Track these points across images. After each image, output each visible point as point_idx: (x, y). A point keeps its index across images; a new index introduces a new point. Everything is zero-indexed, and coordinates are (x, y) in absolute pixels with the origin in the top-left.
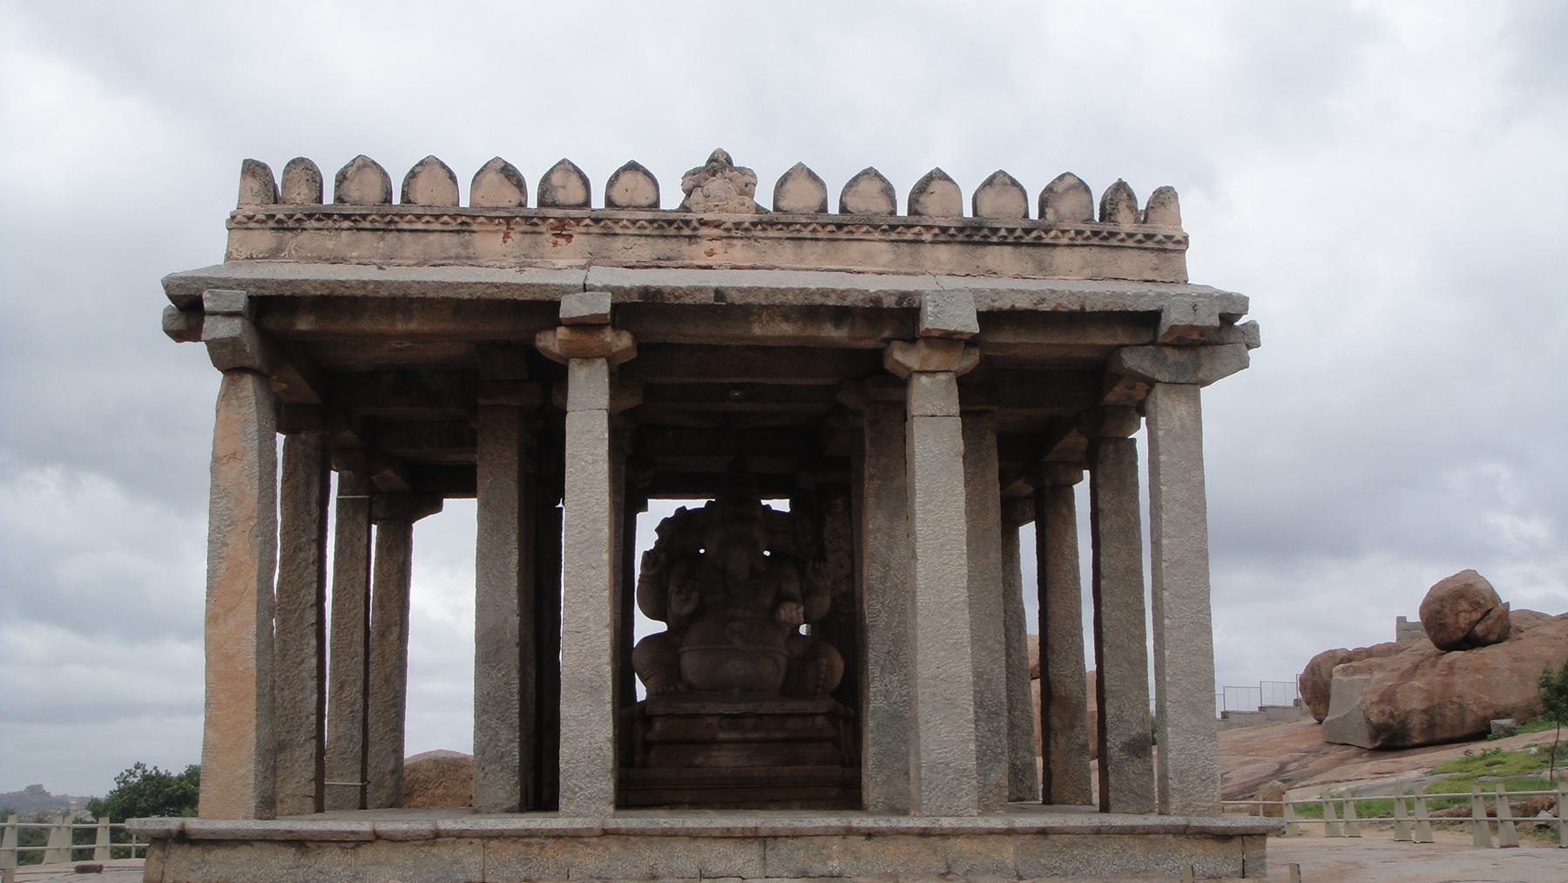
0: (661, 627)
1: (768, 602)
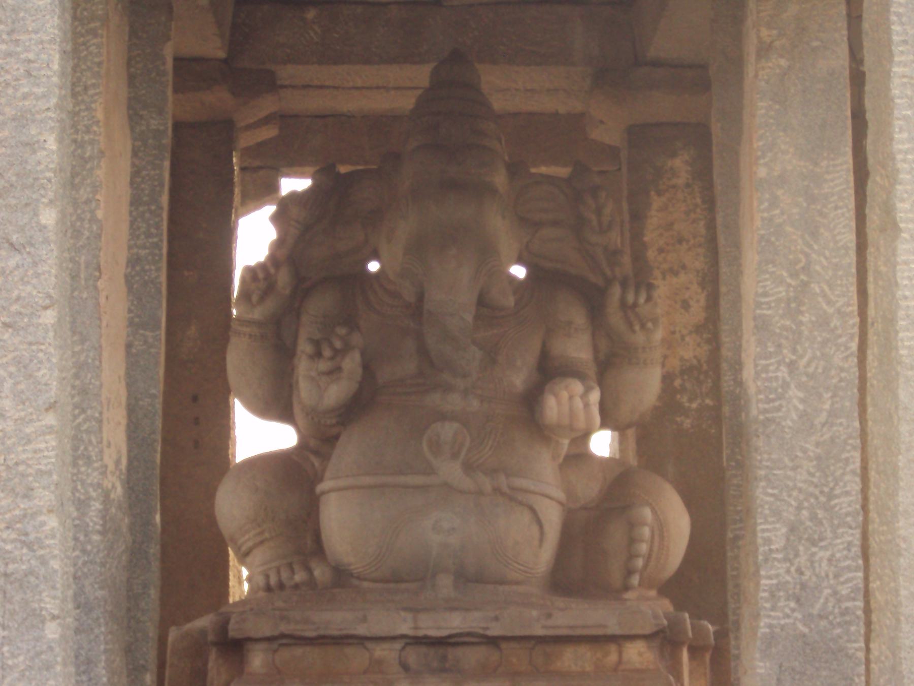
1: (519, 379)
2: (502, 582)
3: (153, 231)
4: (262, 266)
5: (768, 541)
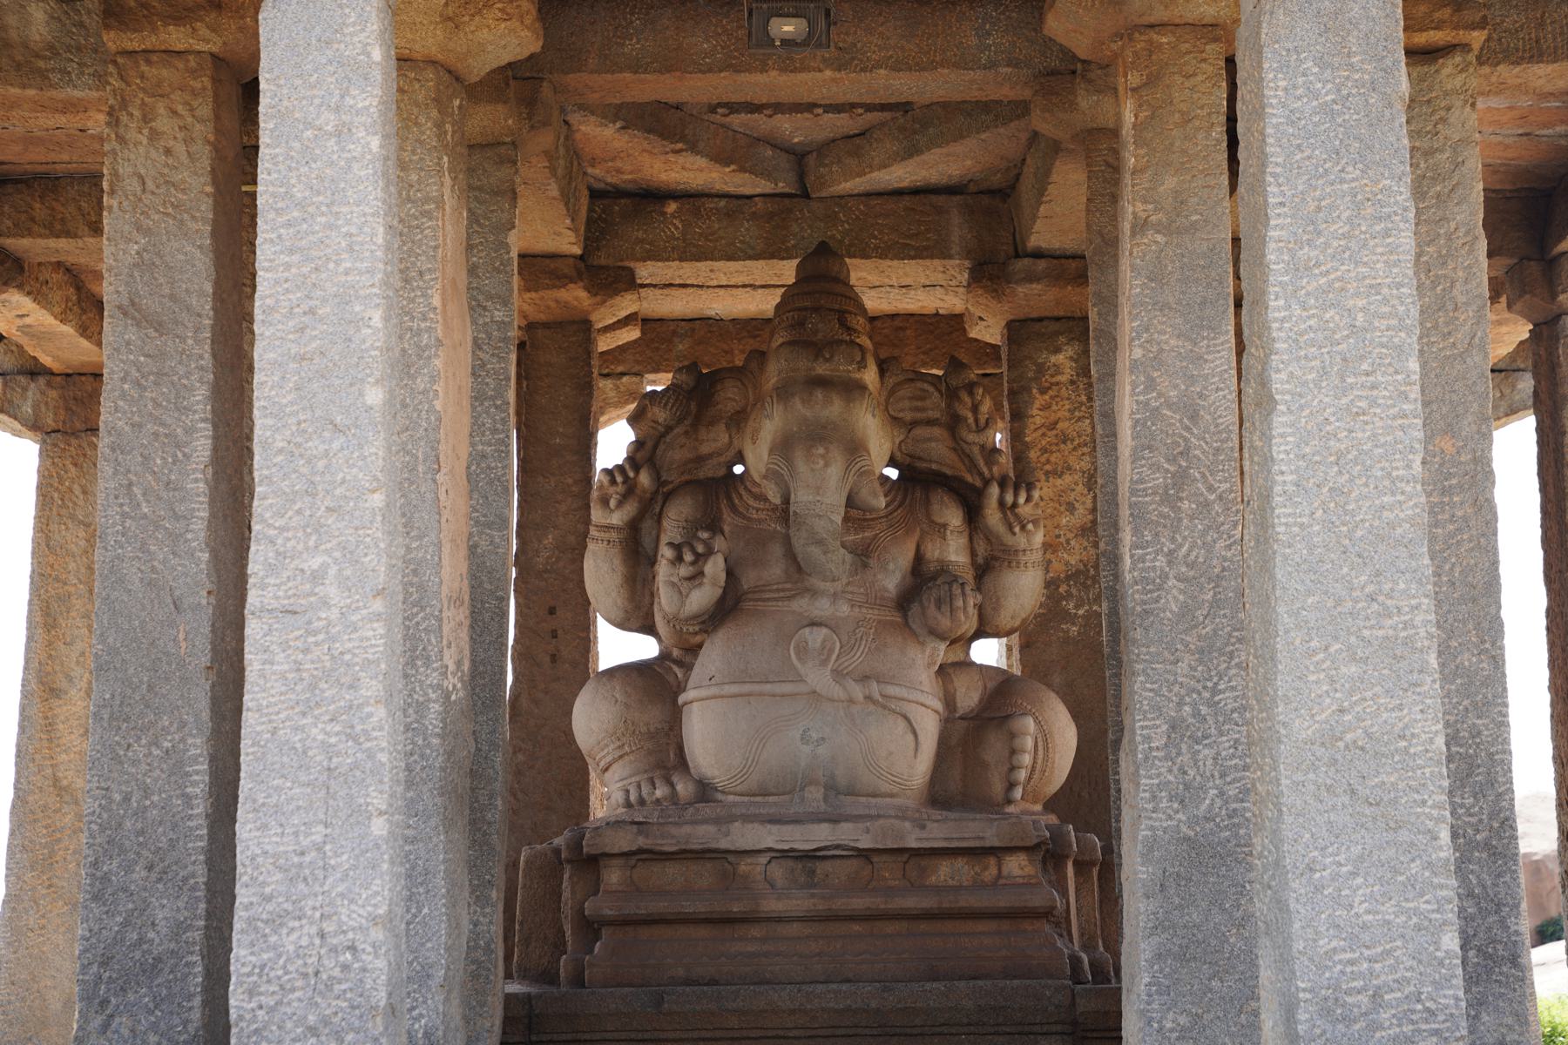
0: (644, 648)
1: (891, 579)
2: (875, 796)
3: (499, 426)
4: (619, 468)
5: (1148, 739)
